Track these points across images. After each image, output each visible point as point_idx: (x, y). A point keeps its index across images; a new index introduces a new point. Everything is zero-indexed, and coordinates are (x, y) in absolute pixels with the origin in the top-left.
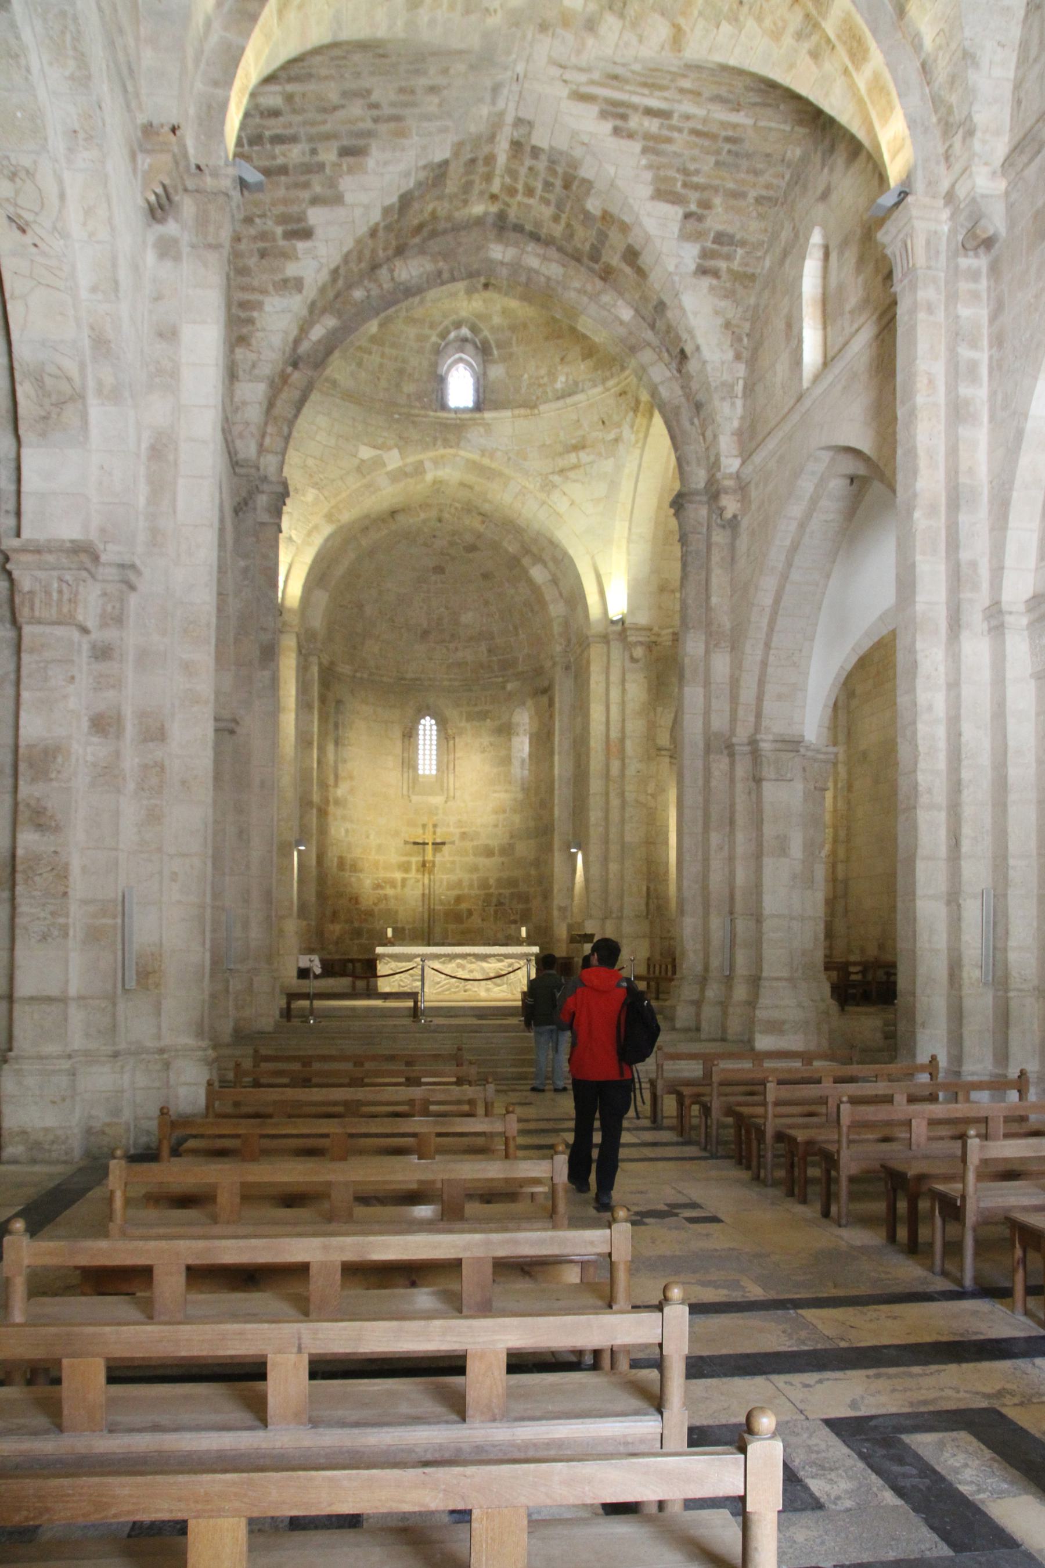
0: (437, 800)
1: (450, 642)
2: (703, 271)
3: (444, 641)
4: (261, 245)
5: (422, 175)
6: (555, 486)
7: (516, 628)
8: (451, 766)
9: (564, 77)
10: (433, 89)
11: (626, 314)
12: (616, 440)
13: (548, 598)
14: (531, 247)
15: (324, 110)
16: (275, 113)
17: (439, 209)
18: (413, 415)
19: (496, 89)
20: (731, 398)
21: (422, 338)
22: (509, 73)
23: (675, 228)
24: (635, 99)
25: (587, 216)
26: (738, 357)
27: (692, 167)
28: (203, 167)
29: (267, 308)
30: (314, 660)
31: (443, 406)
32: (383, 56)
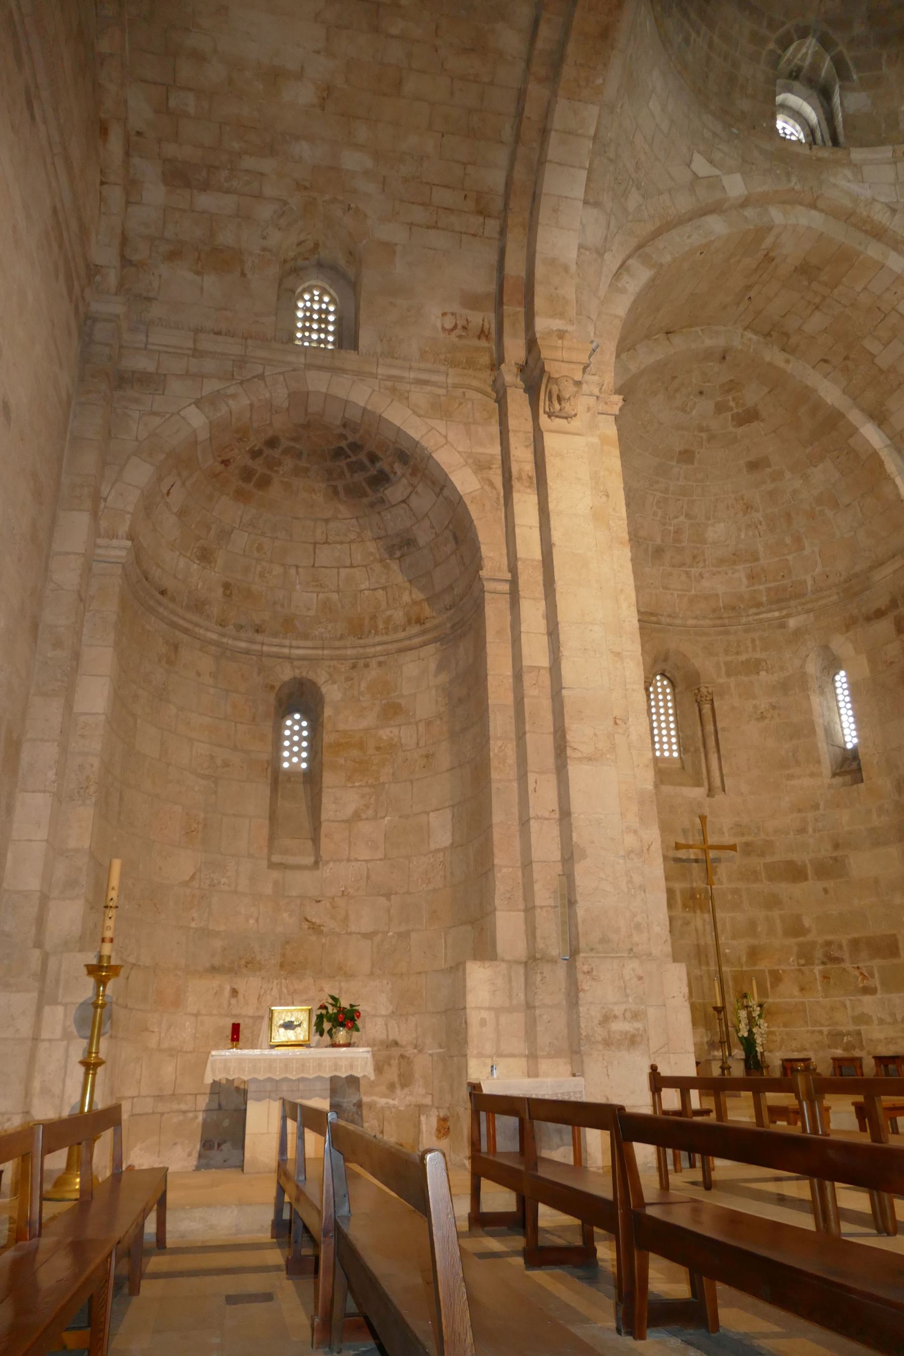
1: (691, 566)
3: (684, 564)
7: (798, 540)
8: (711, 743)
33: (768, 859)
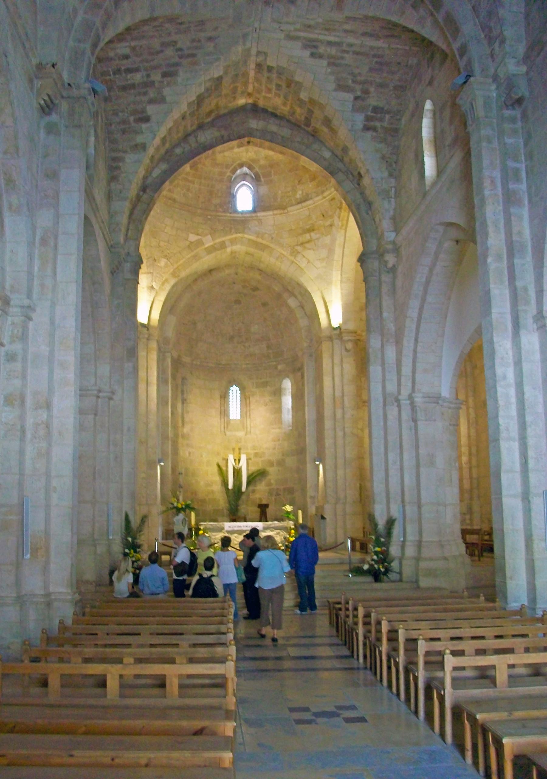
0: (241, 434)
2: (366, 128)
4: (123, 127)
5: (208, 84)
6: (298, 252)
8: (248, 414)
9: (282, 28)
10: (210, 39)
11: (327, 154)
12: (331, 226)
13: (298, 316)
14: (273, 120)
15: (152, 54)
16: (127, 57)
17: (220, 103)
18: (219, 216)
19: (245, 36)
20: (388, 198)
21: (221, 174)
22: (251, 28)
23: (349, 106)
24: (321, 37)
25: (301, 103)
26: (391, 175)
27: (356, 71)
28: (72, 84)
29: (128, 160)
30: (168, 355)
31: (235, 211)
32: (181, 24)
33: (263, 459)
